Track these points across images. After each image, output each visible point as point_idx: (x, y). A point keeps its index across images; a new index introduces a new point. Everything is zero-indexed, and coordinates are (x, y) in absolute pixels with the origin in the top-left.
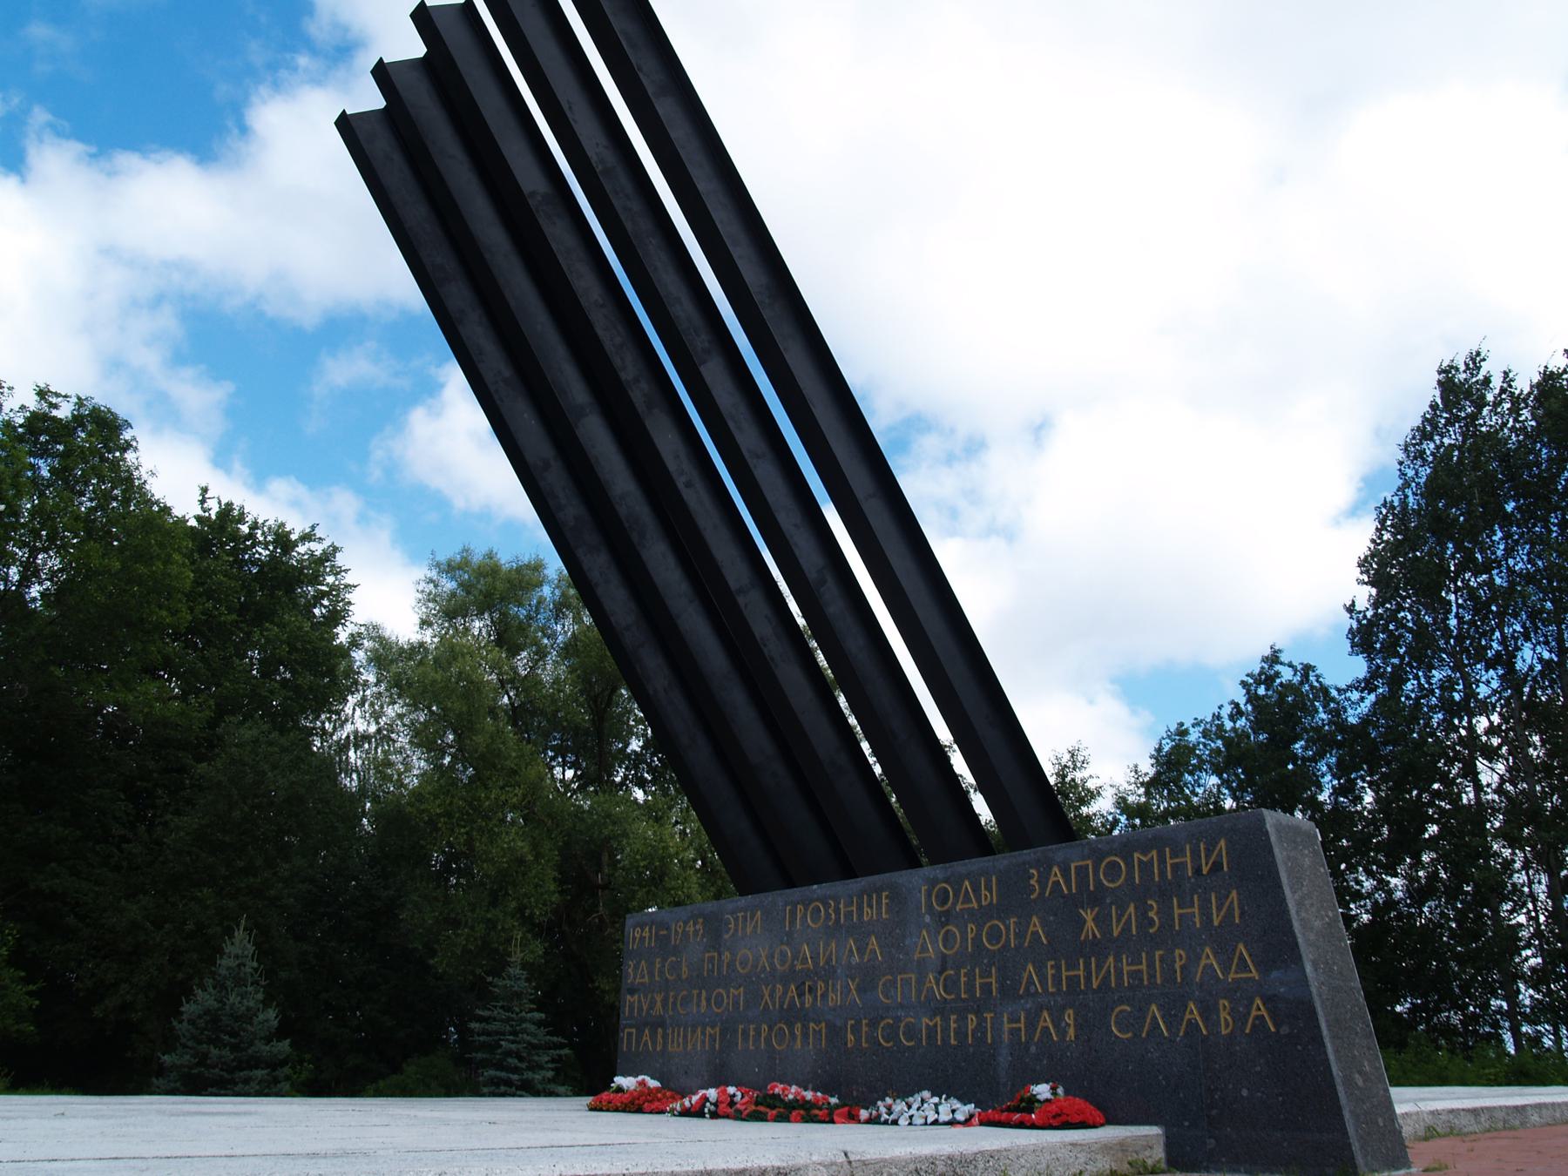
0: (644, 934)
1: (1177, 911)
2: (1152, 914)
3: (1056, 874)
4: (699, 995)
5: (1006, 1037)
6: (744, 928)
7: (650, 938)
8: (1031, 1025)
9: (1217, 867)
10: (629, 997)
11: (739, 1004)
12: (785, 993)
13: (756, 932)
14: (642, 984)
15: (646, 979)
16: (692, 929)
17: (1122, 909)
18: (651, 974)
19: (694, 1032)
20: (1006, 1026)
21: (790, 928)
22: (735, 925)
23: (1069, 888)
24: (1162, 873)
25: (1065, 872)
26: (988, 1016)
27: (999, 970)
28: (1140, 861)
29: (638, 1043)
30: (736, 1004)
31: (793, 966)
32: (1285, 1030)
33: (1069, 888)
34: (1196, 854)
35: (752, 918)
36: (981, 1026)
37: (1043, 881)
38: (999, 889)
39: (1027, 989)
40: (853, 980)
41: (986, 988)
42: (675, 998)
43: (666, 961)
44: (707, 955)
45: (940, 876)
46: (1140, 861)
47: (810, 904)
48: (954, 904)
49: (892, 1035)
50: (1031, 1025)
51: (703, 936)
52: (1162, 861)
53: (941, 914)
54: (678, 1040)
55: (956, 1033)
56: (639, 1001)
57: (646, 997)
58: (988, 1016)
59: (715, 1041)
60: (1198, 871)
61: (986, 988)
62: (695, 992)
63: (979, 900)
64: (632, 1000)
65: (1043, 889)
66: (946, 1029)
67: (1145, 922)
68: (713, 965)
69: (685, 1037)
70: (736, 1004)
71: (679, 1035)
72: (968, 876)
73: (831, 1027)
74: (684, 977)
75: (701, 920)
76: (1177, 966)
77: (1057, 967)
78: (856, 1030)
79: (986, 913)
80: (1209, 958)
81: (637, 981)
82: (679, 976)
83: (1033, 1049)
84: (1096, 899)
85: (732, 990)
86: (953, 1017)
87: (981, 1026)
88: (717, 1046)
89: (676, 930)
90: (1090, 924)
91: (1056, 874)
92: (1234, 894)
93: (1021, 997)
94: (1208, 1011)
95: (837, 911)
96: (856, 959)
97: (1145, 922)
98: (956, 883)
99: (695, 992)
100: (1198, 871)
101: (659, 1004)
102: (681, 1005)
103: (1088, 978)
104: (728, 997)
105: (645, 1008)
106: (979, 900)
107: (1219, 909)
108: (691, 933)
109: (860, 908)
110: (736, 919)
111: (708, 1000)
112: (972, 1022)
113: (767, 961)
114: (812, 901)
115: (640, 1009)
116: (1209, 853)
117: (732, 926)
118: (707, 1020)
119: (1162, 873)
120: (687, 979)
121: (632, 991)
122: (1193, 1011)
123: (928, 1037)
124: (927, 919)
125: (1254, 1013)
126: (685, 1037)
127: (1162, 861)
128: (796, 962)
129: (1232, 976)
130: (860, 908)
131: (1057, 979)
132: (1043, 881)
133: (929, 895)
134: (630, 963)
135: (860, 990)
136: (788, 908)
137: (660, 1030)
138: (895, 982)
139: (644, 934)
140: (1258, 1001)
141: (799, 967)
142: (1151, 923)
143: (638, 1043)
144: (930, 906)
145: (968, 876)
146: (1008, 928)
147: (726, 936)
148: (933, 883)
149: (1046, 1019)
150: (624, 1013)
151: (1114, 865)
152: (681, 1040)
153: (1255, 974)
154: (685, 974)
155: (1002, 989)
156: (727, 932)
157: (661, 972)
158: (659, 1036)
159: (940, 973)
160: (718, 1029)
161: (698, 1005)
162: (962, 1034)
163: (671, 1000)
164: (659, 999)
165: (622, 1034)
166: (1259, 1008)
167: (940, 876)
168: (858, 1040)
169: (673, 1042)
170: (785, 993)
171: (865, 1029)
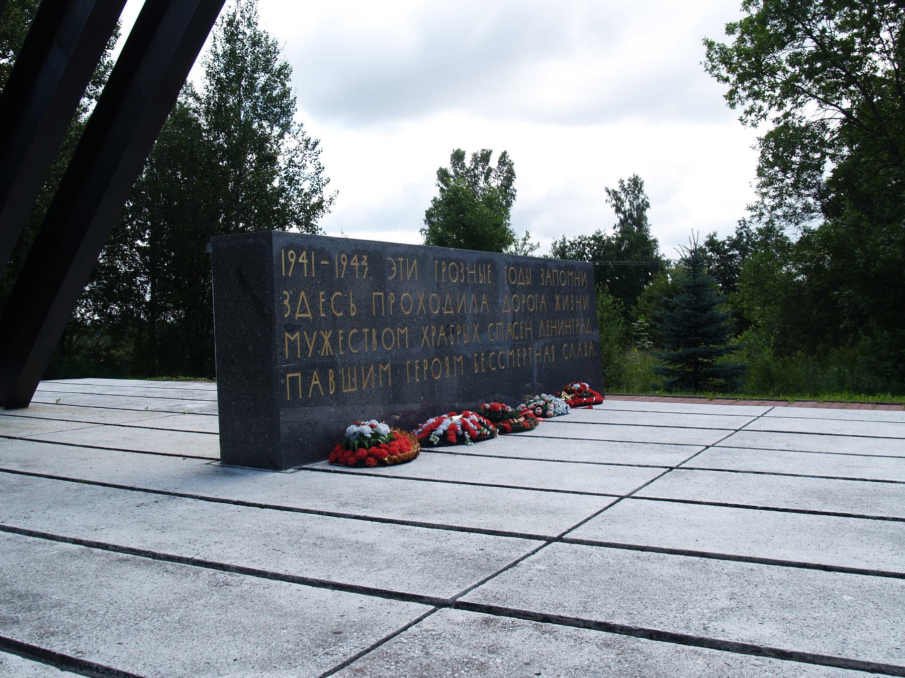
4: (370, 334)
6: (405, 273)
10: (287, 334)
11: (405, 342)
12: (438, 333)
13: (414, 279)
14: (304, 319)
16: (357, 264)
18: (315, 310)
19: (367, 370)
21: (438, 280)
22: (397, 269)
26: (530, 349)
29: (306, 390)
30: (403, 341)
35: (410, 265)
38: (532, 276)
42: (345, 336)
43: (331, 295)
44: (375, 294)
51: (369, 275)
54: (351, 380)
56: (303, 340)
57: (310, 335)
58: (530, 349)
59: (387, 377)
62: (366, 330)
64: (292, 339)
68: (381, 304)
69: (359, 376)
70: (403, 341)
71: (352, 373)
73: (465, 358)
74: (353, 314)
75: (365, 257)
81: (298, 315)
82: (347, 313)
85: (398, 329)
88: (390, 382)
89: (339, 260)
93: (540, 338)
101: (327, 342)
102: (352, 343)
104: (396, 336)
105: (311, 348)
108: (357, 268)
110: (398, 263)
111: (379, 337)
113: (424, 305)
114: (451, 261)
115: (305, 349)
117: (394, 269)
118: (379, 358)
120: (355, 316)
121: (292, 329)
126: (359, 376)
128: (443, 309)
134: (285, 292)
136: (436, 262)
139: (300, 261)
143: (306, 390)
147: (390, 278)
150: (282, 354)
152: (355, 380)
156: (391, 275)
157: (326, 307)
158: (331, 379)
161: (370, 344)
163: (341, 338)
164: (326, 338)
165: (283, 382)
169: (346, 382)
170: (438, 333)
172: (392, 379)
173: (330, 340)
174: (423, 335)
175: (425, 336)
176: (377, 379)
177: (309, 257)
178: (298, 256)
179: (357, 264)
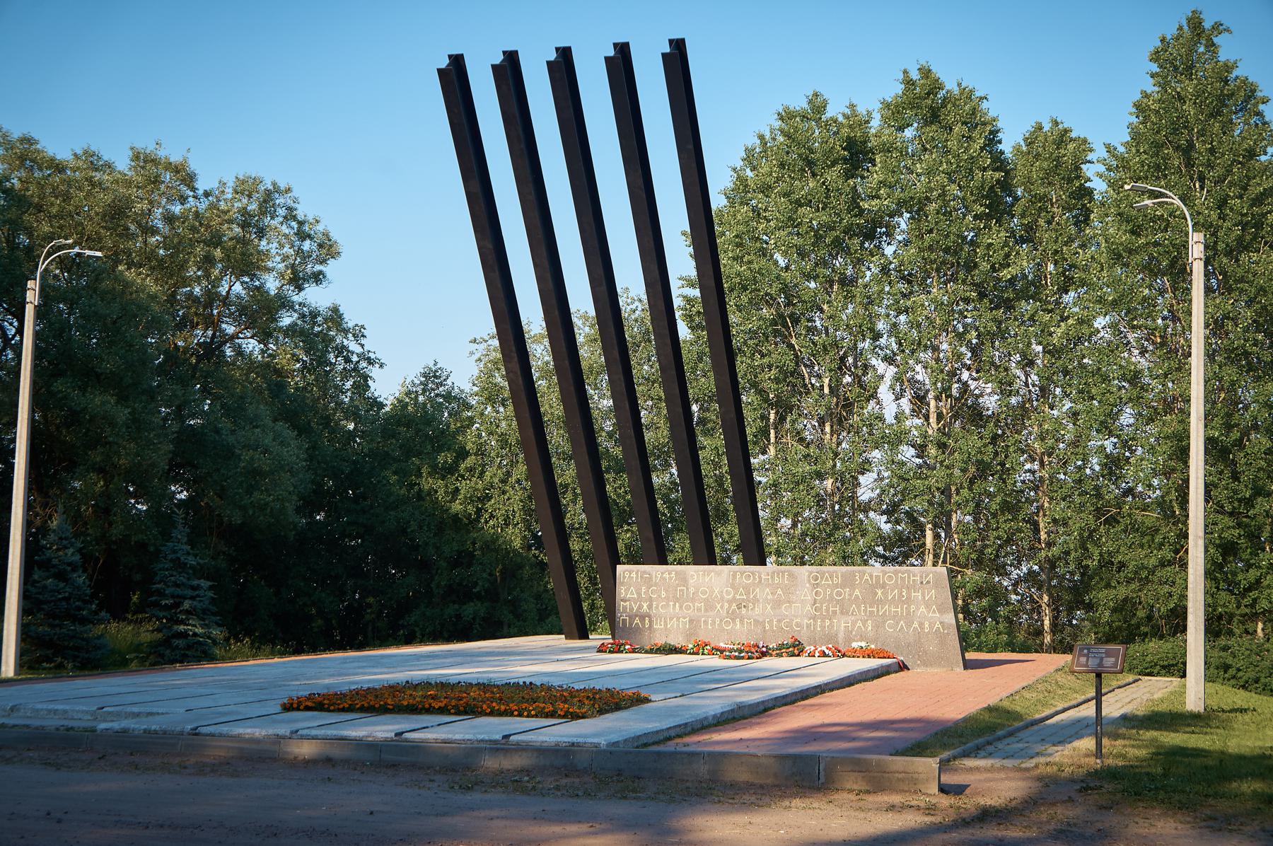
2: (904, 594)
3: (867, 577)
4: (674, 605)
5: (843, 628)
7: (637, 578)
8: (854, 623)
9: (928, 582)
12: (730, 607)
17: (893, 591)
18: (639, 594)
20: (843, 625)
25: (871, 576)
29: (631, 624)
34: (921, 577)
35: (708, 575)
37: (861, 578)
39: (852, 614)
49: (789, 625)
50: (854, 623)
51: (675, 580)
52: (909, 577)
55: (820, 627)
62: (671, 603)
65: (861, 580)
67: (901, 595)
71: (661, 621)
72: (828, 572)
78: (771, 622)
79: (837, 586)
80: (923, 609)
83: (854, 633)
84: (883, 586)
87: (831, 625)
94: (921, 624)
95: (760, 577)
97: (901, 595)
98: (824, 573)
99: (671, 603)
100: (922, 583)
101: (645, 607)
103: (878, 611)
109: (772, 577)
110: (698, 575)
111: (681, 607)
112: (827, 623)
114: (745, 572)
121: (625, 601)
122: (916, 625)
123: (807, 627)
124: (808, 585)
126: (665, 622)
127: (909, 577)
131: (865, 611)
132: (861, 578)
138: (790, 607)
141: (738, 597)
142: (903, 596)
146: (845, 593)
148: (811, 573)
149: (859, 624)
150: (619, 610)
152: (662, 623)
154: (663, 594)
155: (842, 613)
158: (647, 621)
166: (938, 625)
168: (771, 627)
170: (730, 607)
176: (678, 625)
177: (637, 573)
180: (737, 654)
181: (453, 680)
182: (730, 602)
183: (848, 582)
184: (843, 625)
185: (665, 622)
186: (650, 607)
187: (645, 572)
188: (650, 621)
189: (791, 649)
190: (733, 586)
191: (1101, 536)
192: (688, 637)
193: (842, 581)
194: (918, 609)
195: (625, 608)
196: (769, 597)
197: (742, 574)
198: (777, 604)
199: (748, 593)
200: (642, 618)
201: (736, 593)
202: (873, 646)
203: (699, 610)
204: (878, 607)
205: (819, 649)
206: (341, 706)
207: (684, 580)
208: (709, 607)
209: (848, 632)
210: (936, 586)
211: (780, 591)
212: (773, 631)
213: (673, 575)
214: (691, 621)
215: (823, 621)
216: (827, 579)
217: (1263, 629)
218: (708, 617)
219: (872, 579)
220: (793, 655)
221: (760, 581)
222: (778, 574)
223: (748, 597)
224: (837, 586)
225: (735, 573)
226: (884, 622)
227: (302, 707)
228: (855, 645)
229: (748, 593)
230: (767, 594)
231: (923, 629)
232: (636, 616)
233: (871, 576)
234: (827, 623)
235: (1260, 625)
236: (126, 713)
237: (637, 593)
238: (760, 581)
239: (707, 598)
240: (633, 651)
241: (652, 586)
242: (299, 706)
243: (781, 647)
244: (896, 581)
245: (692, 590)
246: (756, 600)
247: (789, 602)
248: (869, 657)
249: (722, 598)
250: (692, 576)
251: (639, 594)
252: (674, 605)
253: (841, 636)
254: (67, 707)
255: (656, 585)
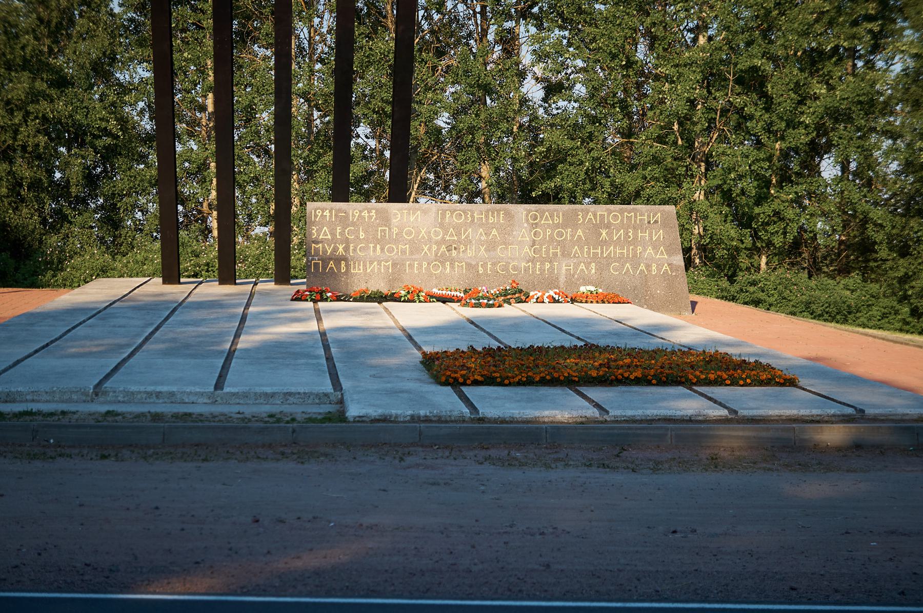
0: (325, 214)
1: (640, 234)
2: (630, 234)
3: (590, 215)
4: (375, 247)
5: (564, 272)
7: (331, 216)
8: (576, 268)
9: (656, 222)
12: (438, 249)
15: (329, 237)
17: (618, 231)
18: (333, 235)
20: (564, 268)
23: (596, 221)
24: (635, 221)
25: (595, 215)
27: (561, 247)
28: (627, 216)
29: (324, 268)
31: (443, 237)
32: (674, 274)
33: (596, 221)
34: (649, 216)
35: (414, 214)
36: (552, 268)
39: (574, 255)
40: (482, 245)
41: (555, 254)
44: (380, 228)
45: (533, 209)
46: (627, 216)
47: (454, 212)
48: (540, 221)
49: (505, 269)
50: (576, 268)
51: (376, 219)
52: (636, 217)
53: (532, 224)
55: (540, 270)
60: (649, 222)
61: (555, 254)
62: (371, 245)
63: (553, 220)
65: (584, 220)
66: (534, 267)
71: (359, 265)
72: (547, 211)
76: (638, 252)
77: (589, 249)
78: (484, 266)
79: (557, 226)
80: (650, 250)
81: (321, 237)
83: (576, 276)
84: (608, 226)
86: (538, 263)
87: (552, 268)
89: (353, 214)
90: (604, 234)
91: (590, 215)
92: (661, 231)
95: (472, 216)
96: (484, 238)
99: (371, 245)
100: (649, 222)
103: (602, 252)
104: (397, 249)
106: (553, 220)
107: (655, 235)
109: (487, 217)
110: (402, 215)
111: (382, 249)
112: (547, 266)
114: (455, 211)
115: (325, 251)
116: (654, 217)
119: (635, 221)
121: (316, 242)
122: (642, 267)
124: (526, 225)
125: (664, 268)
126: (365, 266)
127: (636, 217)
129: (658, 256)
130: (487, 217)
132: (584, 218)
133: (527, 216)
135: (486, 250)
137: (343, 264)
139: (325, 214)
140: (666, 265)
141: (448, 238)
142: (629, 237)
144: (527, 220)
145: (547, 211)
147: (394, 221)
148: (529, 211)
149: (582, 266)
151: (615, 216)
152: (361, 267)
153: (666, 257)
154: (362, 235)
155: (563, 255)
158: (343, 266)
159: (532, 247)
160: (390, 263)
162: (542, 270)
163: (351, 248)
167: (533, 209)
170: (438, 249)
171: (489, 266)
172: (392, 270)
173: (343, 248)
174: (423, 250)
175: (426, 249)
176: (379, 269)
177: (331, 212)
178: (323, 212)
179: (367, 215)
180: (486, 301)
181: (282, 339)
182: (439, 244)
183: (570, 222)
184: (564, 268)
185: (365, 266)
186: (346, 249)
187: (340, 210)
188: (347, 266)
189: (517, 295)
190: (441, 225)
191: (610, 167)
192: (392, 280)
193: (563, 220)
194: (645, 250)
195: (317, 250)
196: (483, 238)
197: (452, 212)
198: (491, 246)
199: (459, 234)
200: (338, 260)
201: (446, 233)
202: (600, 291)
203: (403, 252)
204: (602, 249)
205: (547, 294)
206: (517, 379)
207: (385, 220)
208: (415, 248)
209: (570, 276)
210: (665, 225)
211: (494, 232)
212: (488, 275)
213: (373, 213)
214: (394, 265)
215: (542, 264)
216: (547, 219)
217: (767, 264)
218: (414, 260)
219: (595, 218)
220: (521, 302)
221: (473, 221)
222: (493, 213)
223: (459, 238)
224: (557, 226)
225: (444, 212)
226: (609, 265)
227: (469, 382)
228: (583, 289)
229: (459, 234)
230: (481, 234)
231: (650, 271)
232: (330, 259)
233: (595, 215)
234: (547, 266)
235: (764, 260)
236: (256, 393)
237: (331, 234)
238: (473, 221)
239: (413, 240)
240: (338, 299)
241: (348, 226)
242: (465, 380)
243: (505, 293)
244: (622, 220)
245: (395, 230)
246: (468, 242)
247: (505, 243)
248: (603, 302)
249: (430, 239)
250: (396, 214)
251: (333, 235)
252: (375, 247)
253: (562, 279)
254: (174, 389)
255: (353, 224)
